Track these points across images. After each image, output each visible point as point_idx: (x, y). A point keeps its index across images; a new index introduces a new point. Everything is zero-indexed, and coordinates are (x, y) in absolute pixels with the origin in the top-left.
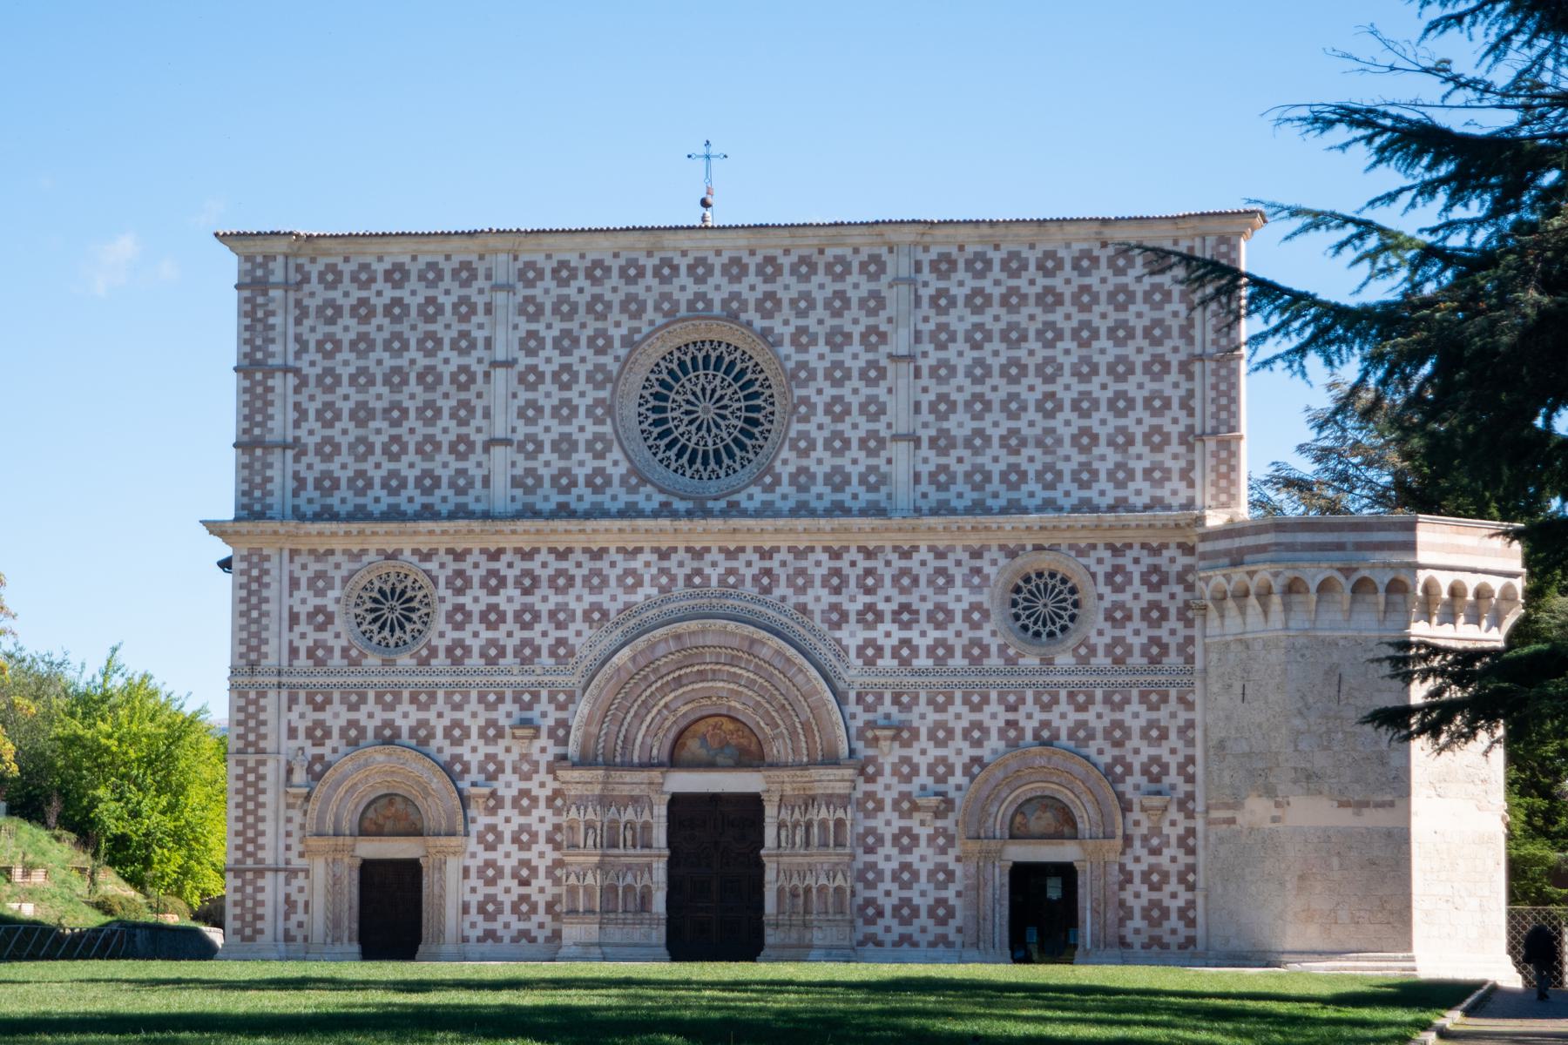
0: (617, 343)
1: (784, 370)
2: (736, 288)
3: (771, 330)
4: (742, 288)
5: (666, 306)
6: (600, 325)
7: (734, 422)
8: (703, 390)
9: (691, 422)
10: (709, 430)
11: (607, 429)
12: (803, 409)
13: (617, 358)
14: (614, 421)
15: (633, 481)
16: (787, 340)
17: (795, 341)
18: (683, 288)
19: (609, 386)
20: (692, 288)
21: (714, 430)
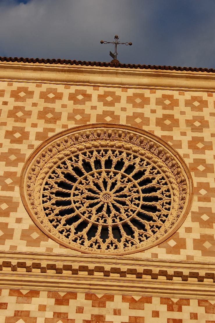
0: (32, 137)
1: (183, 162)
2: (139, 110)
3: (171, 138)
4: (146, 111)
5: (78, 117)
6: (18, 124)
7: (132, 207)
8: (105, 183)
9: (91, 206)
10: (109, 211)
11: (15, 194)
12: (203, 192)
13: (31, 146)
14: (21, 188)
15: (35, 235)
16: (185, 145)
17: (192, 145)
18: (94, 108)
19: (21, 165)
20: (101, 108)
21: (114, 212)
